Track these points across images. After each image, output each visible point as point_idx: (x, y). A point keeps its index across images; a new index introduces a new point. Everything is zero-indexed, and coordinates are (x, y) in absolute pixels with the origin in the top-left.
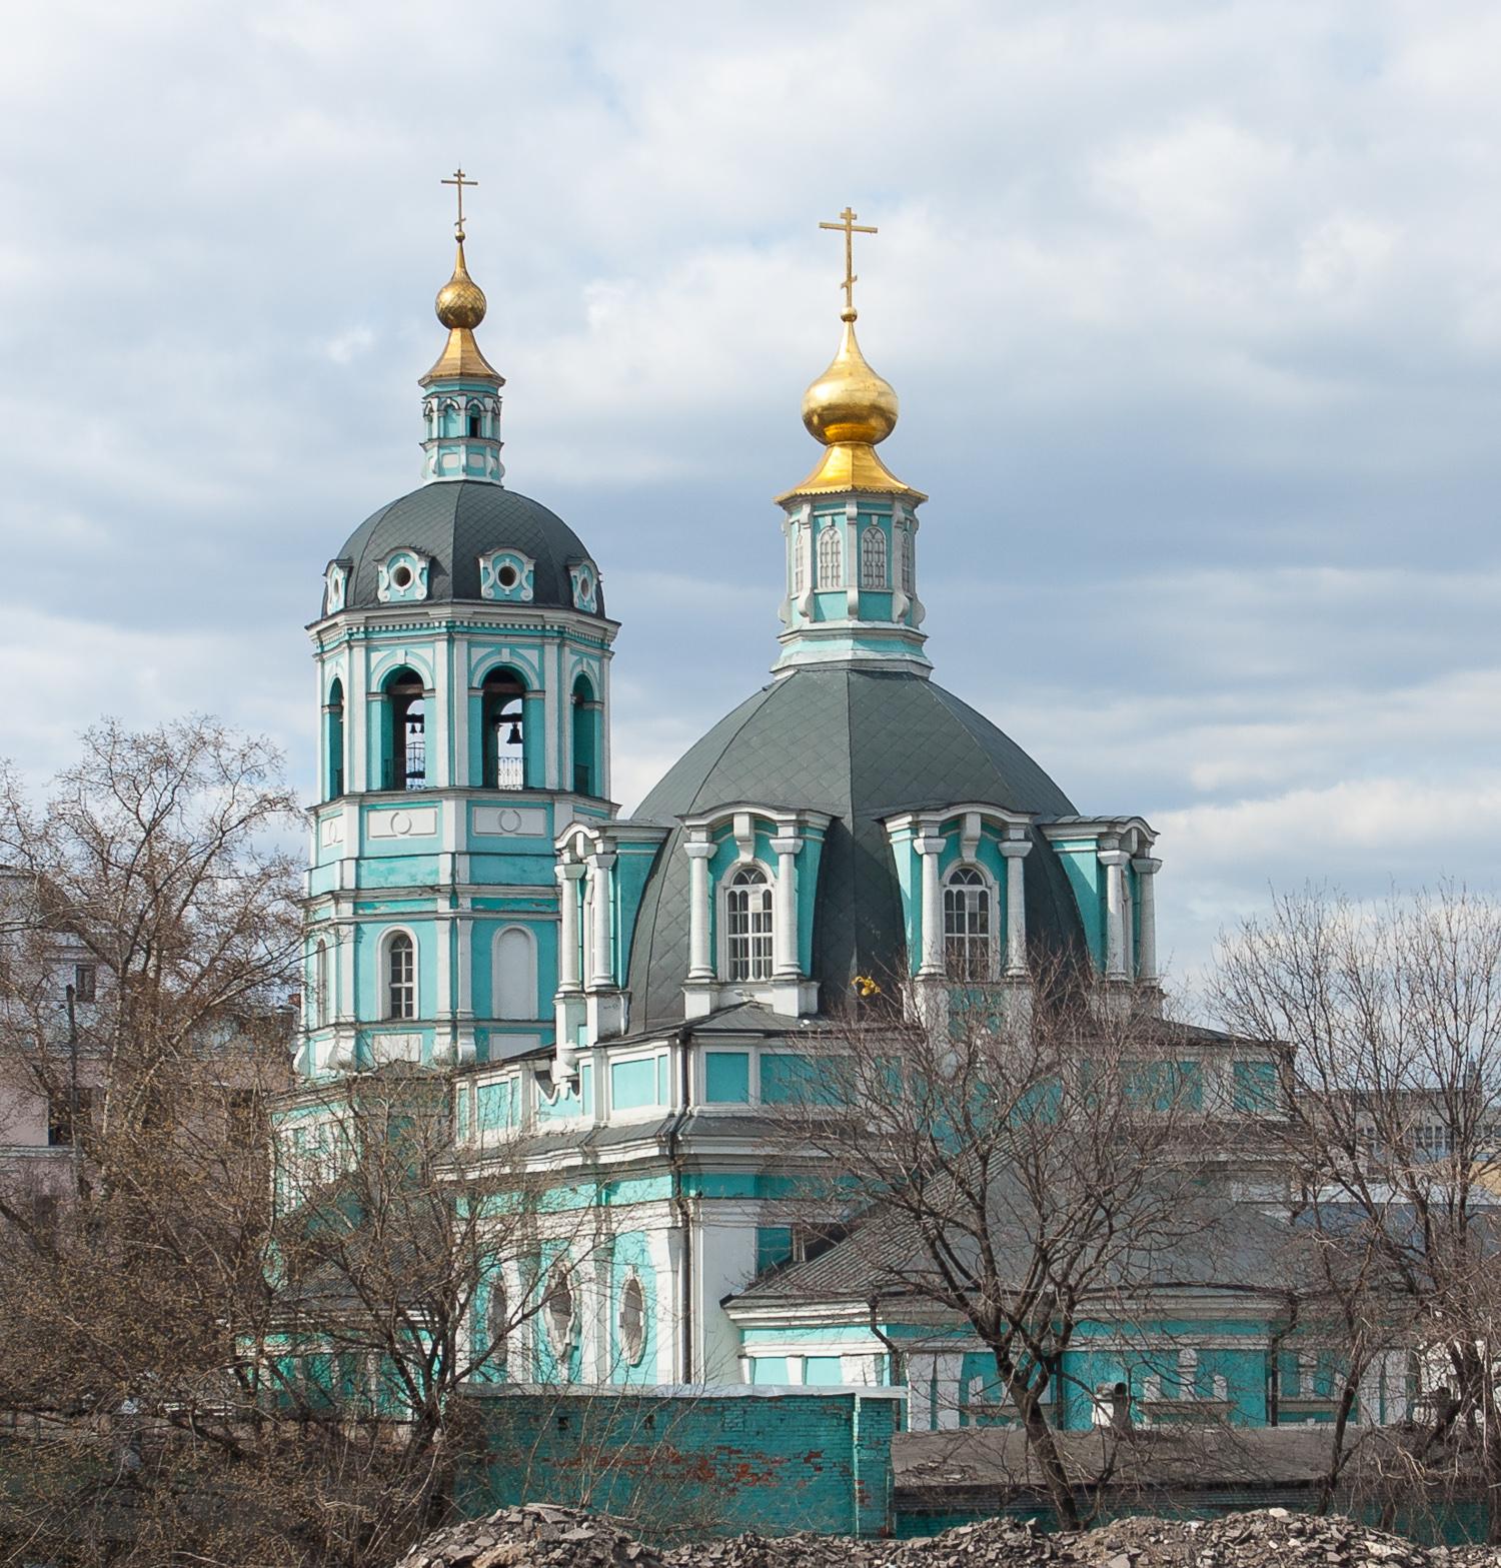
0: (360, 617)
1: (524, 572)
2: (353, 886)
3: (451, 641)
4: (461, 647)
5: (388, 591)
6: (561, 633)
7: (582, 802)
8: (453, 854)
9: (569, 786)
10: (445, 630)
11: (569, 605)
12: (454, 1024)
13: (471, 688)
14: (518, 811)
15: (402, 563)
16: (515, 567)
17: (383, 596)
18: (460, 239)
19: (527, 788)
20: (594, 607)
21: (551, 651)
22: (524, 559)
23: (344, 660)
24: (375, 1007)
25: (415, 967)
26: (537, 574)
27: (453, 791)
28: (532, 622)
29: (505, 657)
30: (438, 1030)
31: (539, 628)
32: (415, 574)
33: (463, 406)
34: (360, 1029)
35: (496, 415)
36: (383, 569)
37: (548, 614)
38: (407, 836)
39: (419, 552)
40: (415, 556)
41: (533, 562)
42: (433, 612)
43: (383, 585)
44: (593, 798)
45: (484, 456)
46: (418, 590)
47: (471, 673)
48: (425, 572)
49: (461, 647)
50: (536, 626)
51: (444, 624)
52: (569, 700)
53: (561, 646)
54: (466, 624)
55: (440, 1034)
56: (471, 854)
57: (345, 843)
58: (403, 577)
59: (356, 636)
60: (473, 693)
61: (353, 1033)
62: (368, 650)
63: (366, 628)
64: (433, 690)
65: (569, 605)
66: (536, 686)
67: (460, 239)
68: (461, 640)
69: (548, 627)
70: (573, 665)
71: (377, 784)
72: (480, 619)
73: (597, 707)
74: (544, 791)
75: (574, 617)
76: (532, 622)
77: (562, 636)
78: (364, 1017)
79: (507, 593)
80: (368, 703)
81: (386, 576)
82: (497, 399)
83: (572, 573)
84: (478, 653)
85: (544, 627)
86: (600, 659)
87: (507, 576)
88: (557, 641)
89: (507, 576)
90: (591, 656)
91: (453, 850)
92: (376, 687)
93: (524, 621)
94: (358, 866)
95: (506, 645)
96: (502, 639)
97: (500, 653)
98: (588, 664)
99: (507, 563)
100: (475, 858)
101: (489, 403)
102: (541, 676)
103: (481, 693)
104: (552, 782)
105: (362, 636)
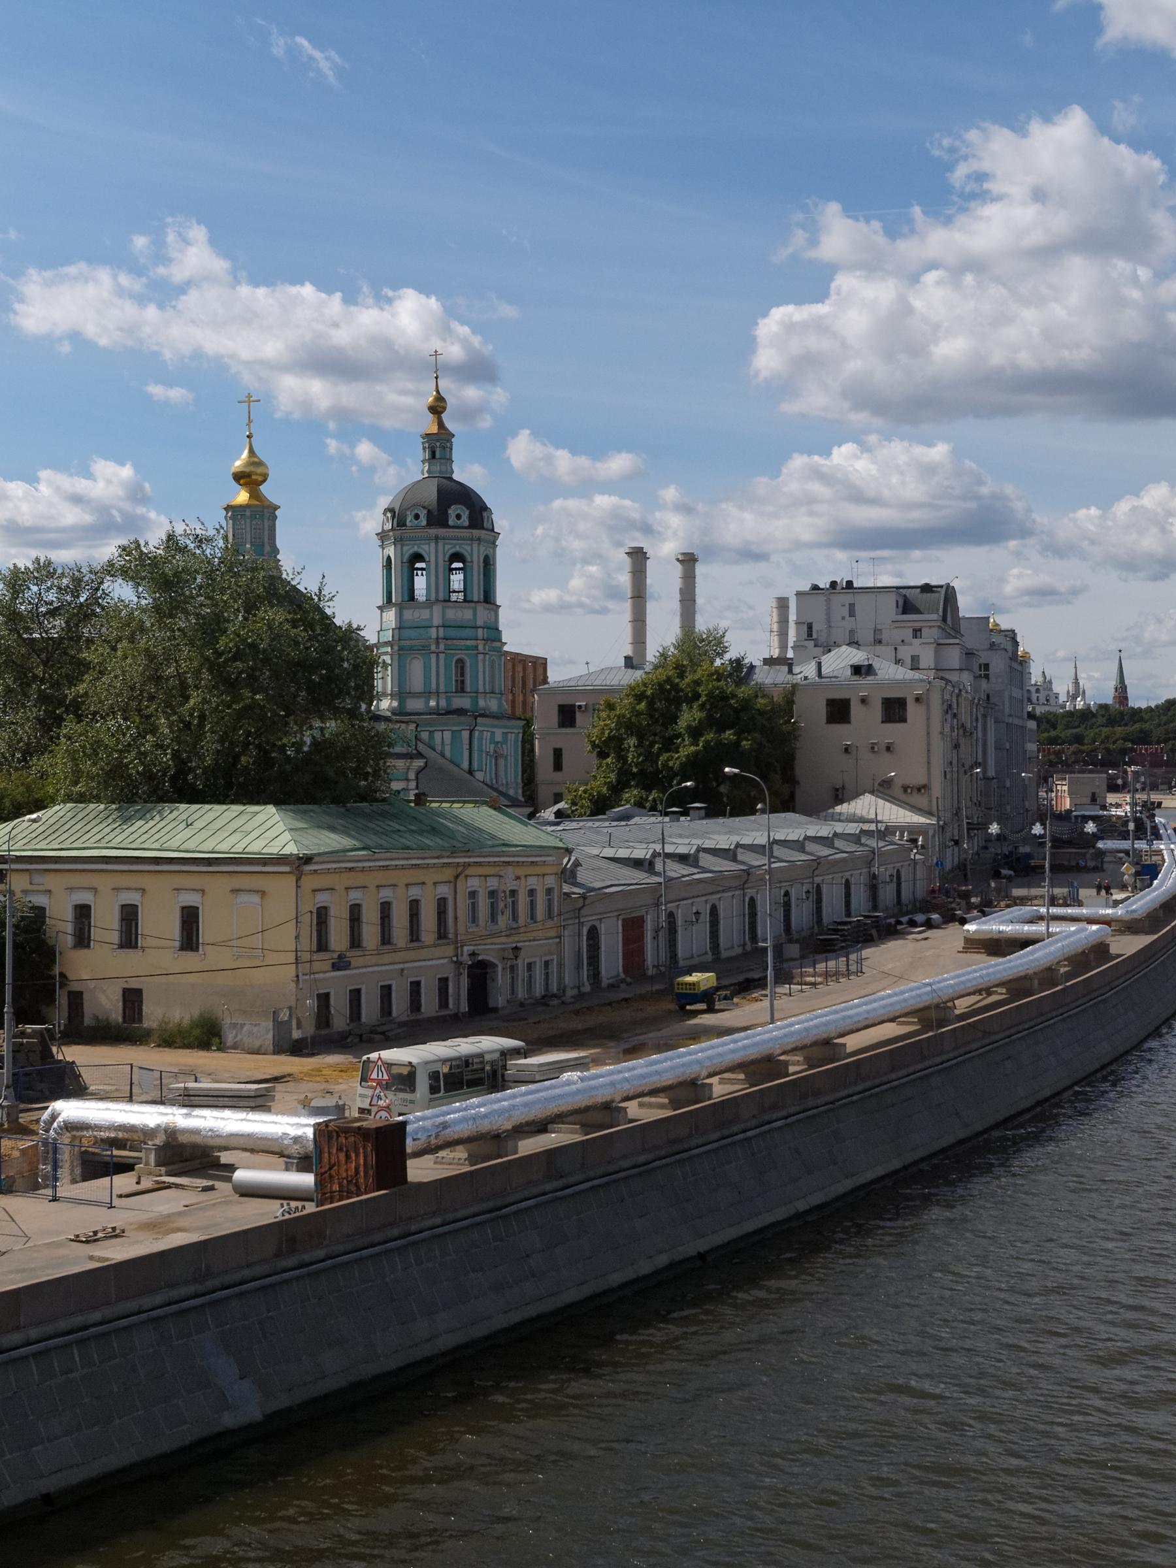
7: (487, 606)
9: (482, 600)
17: (451, 523)
19: (465, 601)
44: (490, 603)
47: (444, 557)
52: (482, 565)
56: (443, 626)
74: (472, 601)
75: (484, 532)
82: (451, 445)
101: (448, 444)
104: (476, 599)
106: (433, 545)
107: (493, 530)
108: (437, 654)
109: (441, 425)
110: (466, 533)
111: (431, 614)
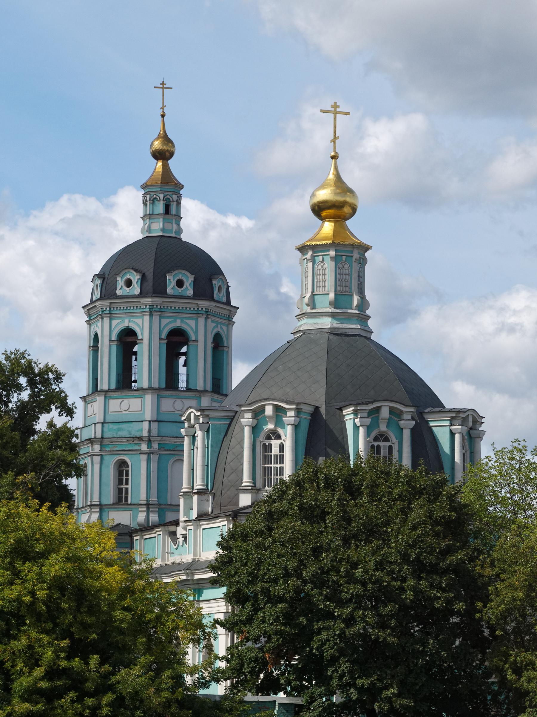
0: (106, 303)
1: (189, 280)
2: (100, 436)
3: (151, 315)
4: (156, 318)
5: (121, 290)
6: (207, 312)
7: (216, 396)
8: (150, 421)
9: (209, 387)
10: (148, 310)
11: (211, 298)
12: (148, 506)
13: (160, 339)
14: (183, 400)
15: (128, 276)
16: (184, 279)
17: (119, 292)
18: (163, 116)
19: (188, 389)
20: (224, 299)
21: (201, 321)
22: (189, 275)
23: (99, 324)
24: (110, 498)
25: (130, 478)
26: (196, 282)
27: (150, 389)
28: (192, 306)
29: (178, 324)
30: (140, 509)
31: (196, 309)
32: (134, 282)
33: (162, 198)
34: (101, 507)
35: (179, 203)
36: (119, 279)
37: (200, 303)
38: (127, 412)
39: (137, 271)
40: (135, 273)
41: (193, 276)
42: (143, 300)
43: (119, 287)
45: (172, 223)
46: (136, 289)
47: (161, 331)
48: (139, 281)
49: (156, 318)
50: (194, 308)
51: (148, 307)
52: (210, 346)
53: (206, 319)
54: (159, 307)
55: (140, 511)
57: (97, 415)
58: (129, 283)
59: (105, 312)
60: (162, 341)
61: (98, 510)
62: (111, 319)
63: (110, 308)
64: (142, 339)
65: (211, 298)
66: (193, 338)
67: (163, 116)
68: (156, 315)
69: (200, 309)
70: (212, 327)
71: (113, 386)
72: (166, 305)
73: (225, 349)
74: (196, 391)
75: (214, 304)
76: (192, 306)
77: (207, 313)
78: (104, 502)
79: (180, 291)
80: (110, 345)
81: (120, 282)
82: (179, 197)
83: (214, 282)
84: (165, 321)
85: (198, 309)
86: (228, 325)
87: (180, 284)
88: (205, 316)
89: (180, 284)
90: (222, 324)
91: (150, 419)
92: (114, 338)
93: (189, 306)
94: (103, 427)
95: (179, 318)
96: (177, 315)
97: (176, 321)
98: (221, 327)
99: (180, 277)
100: (161, 424)
102: (196, 333)
103: (166, 341)
104: (200, 386)
105: (108, 312)
106: (147, 318)
107: (228, 302)
108: (149, 454)
109: (166, 170)
110: (190, 304)
111: (143, 404)
